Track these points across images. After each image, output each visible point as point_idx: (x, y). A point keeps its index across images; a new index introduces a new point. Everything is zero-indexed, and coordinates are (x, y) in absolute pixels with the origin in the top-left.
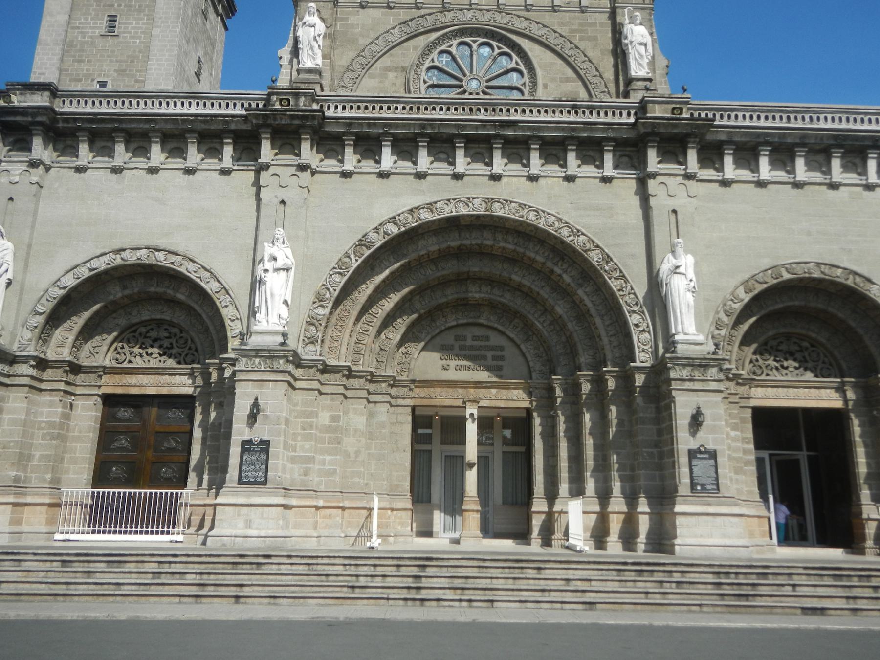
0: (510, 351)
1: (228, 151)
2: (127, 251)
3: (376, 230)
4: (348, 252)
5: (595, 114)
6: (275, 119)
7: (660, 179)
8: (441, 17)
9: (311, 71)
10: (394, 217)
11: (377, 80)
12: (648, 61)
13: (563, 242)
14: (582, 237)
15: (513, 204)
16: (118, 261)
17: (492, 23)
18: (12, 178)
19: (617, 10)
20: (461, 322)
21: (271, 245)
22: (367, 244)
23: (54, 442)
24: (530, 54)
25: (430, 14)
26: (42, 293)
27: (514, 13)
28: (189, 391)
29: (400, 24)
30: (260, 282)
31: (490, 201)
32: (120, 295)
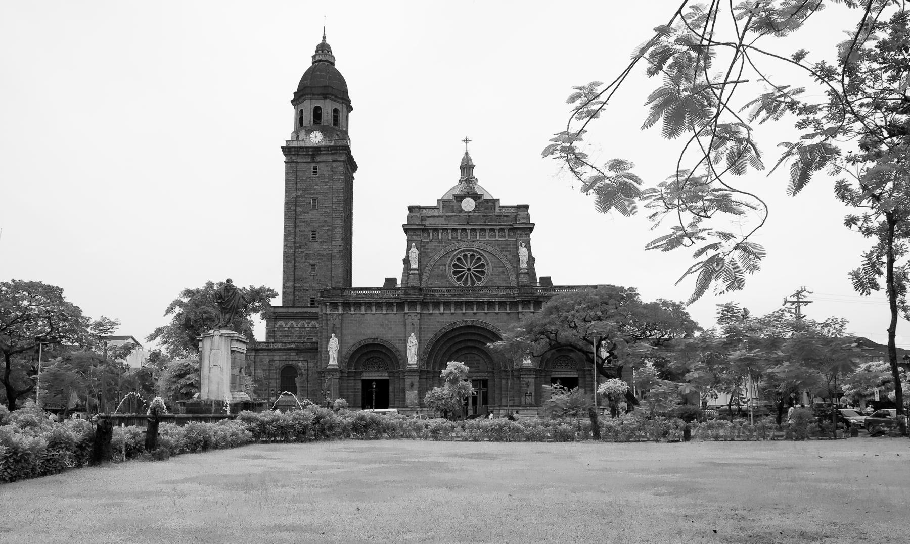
0: (482, 361)
1: (395, 308)
3: (440, 331)
24: (487, 258)
28: (388, 378)
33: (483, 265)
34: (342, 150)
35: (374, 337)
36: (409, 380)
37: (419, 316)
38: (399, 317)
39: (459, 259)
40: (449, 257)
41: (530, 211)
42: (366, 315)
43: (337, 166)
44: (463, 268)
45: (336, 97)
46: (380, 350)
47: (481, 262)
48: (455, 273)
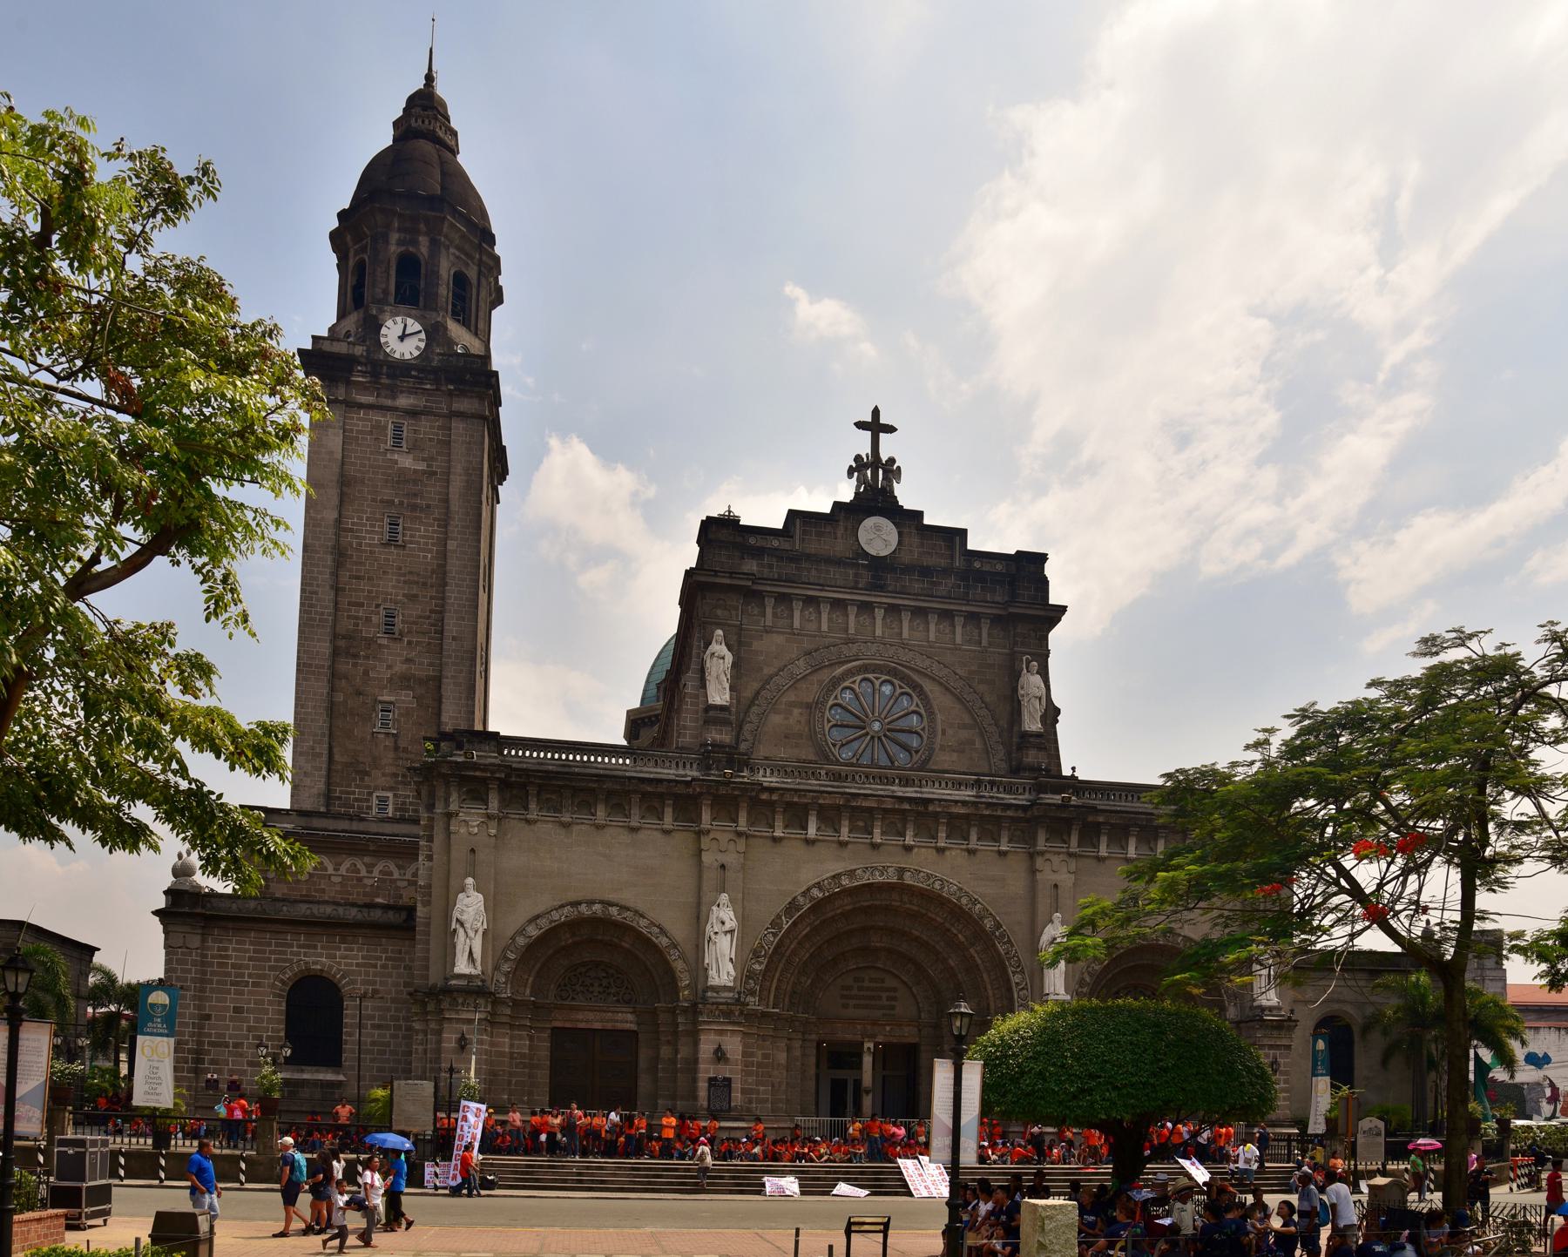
2: (584, 905)
3: (804, 894)
5: (995, 789)
6: (717, 790)
8: (844, 649)
9: (722, 708)
11: (782, 716)
13: (964, 910)
14: (979, 906)
15: (922, 874)
16: (576, 913)
20: (861, 965)
23: (526, 1070)
24: (931, 696)
27: (916, 649)
31: (901, 871)
36: (712, 1037)
37: (742, 842)
38: (682, 840)
41: (1050, 570)
46: (616, 940)
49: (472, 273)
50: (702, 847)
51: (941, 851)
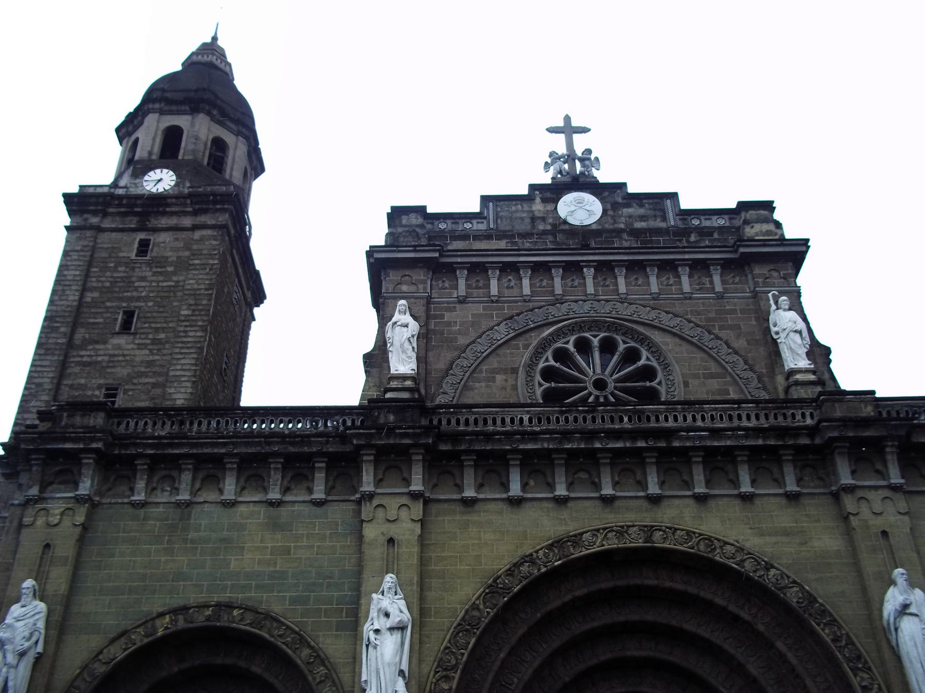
3: (510, 573)
4: (477, 602)
7: (860, 493)
10: (531, 555)
11: (483, 384)
12: (806, 351)
13: (749, 579)
15: (678, 532)
17: (614, 314)
18: (51, 519)
19: (759, 294)
21: (380, 596)
22: (500, 591)
24: (663, 347)
25: (540, 308)
26: (78, 671)
27: (637, 302)
29: (506, 320)
30: (367, 646)
31: (649, 531)
32: (176, 669)
33: (648, 373)
34: (223, 203)
35: (216, 598)
37: (417, 509)
38: (339, 513)
39: (562, 355)
40: (526, 347)
42: (196, 510)
43: (202, 239)
44: (577, 380)
45: (223, 113)
46: (242, 664)
47: (642, 362)
48: (551, 397)
49: (229, 138)
50: (363, 517)
51: (701, 499)
